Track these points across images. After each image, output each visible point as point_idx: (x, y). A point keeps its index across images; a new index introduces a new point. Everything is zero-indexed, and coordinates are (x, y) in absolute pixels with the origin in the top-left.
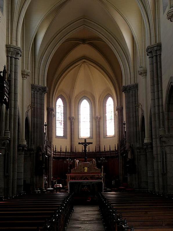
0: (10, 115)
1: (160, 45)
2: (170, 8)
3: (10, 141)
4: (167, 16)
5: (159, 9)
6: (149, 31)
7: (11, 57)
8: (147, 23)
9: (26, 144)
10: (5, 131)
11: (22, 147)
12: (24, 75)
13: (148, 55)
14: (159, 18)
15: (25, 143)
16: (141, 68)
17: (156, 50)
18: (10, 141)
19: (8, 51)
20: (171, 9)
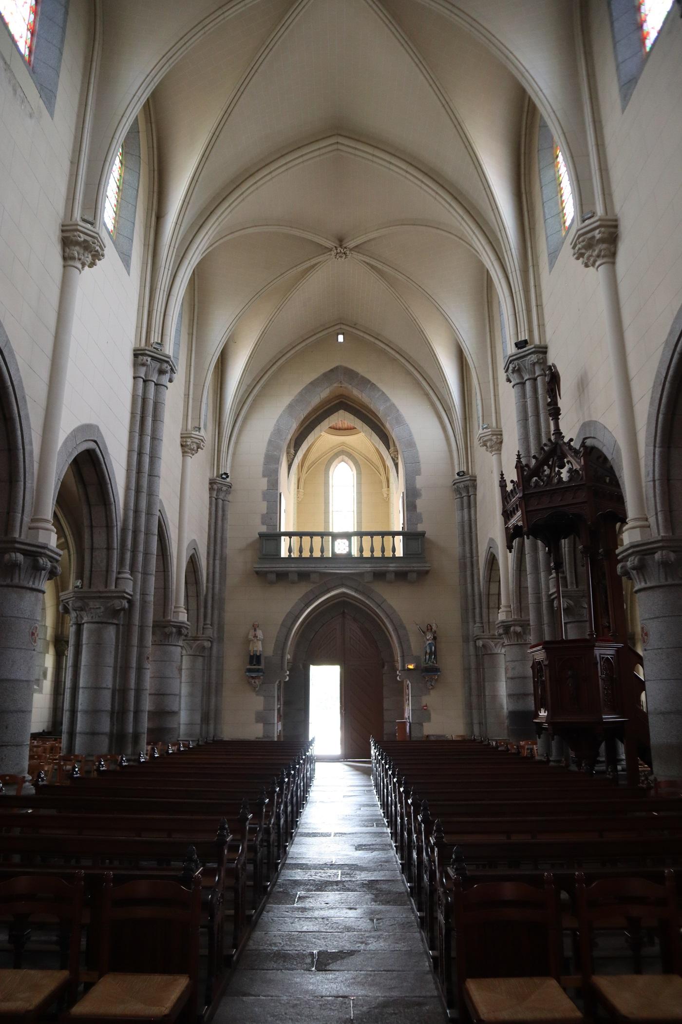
0: (136, 532)
1: (614, 223)
2: (584, 221)
3: (130, 602)
4: (574, 248)
5: (536, 266)
6: (511, 318)
7: (145, 381)
8: (509, 299)
9: (186, 619)
10: (119, 573)
11: (174, 626)
12: (188, 447)
13: (509, 380)
14: (537, 286)
15: (183, 617)
16: (486, 428)
17: (534, 364)
18: (130, 602)
19: (136, 365)
20: (584, 224)
